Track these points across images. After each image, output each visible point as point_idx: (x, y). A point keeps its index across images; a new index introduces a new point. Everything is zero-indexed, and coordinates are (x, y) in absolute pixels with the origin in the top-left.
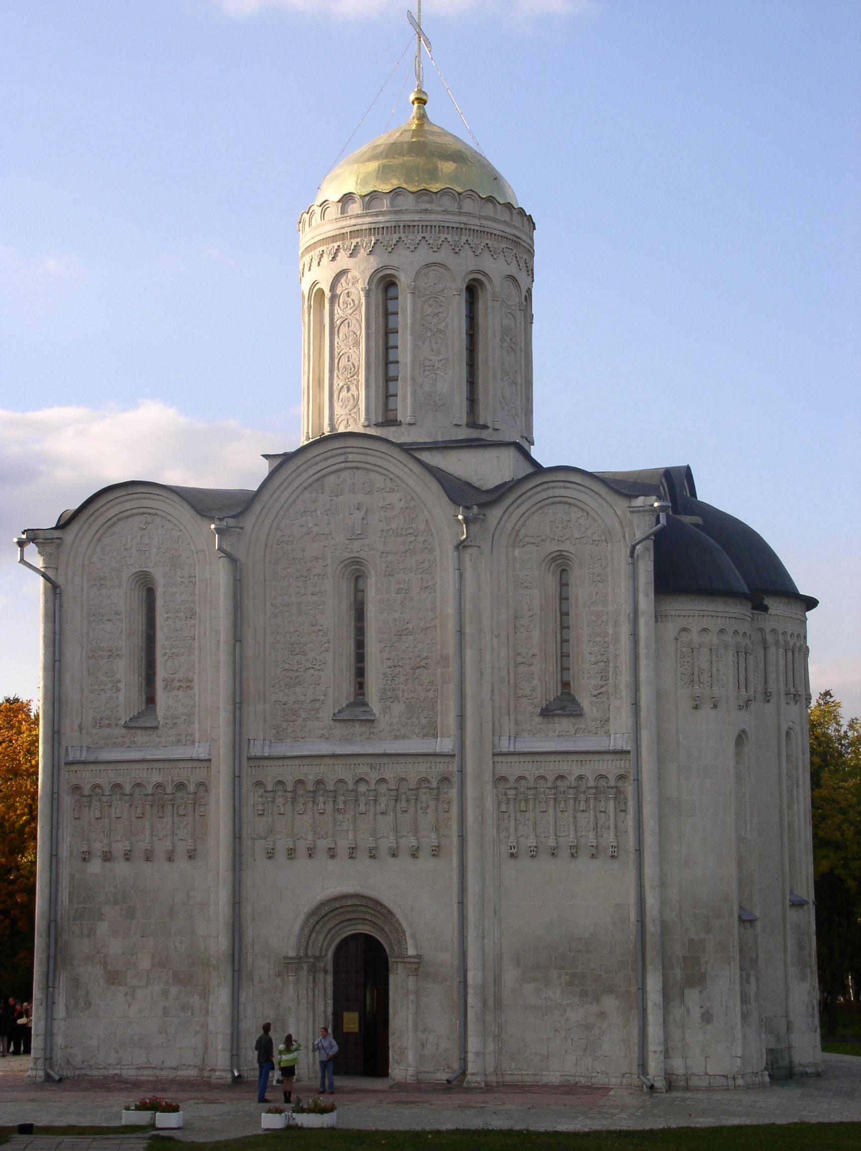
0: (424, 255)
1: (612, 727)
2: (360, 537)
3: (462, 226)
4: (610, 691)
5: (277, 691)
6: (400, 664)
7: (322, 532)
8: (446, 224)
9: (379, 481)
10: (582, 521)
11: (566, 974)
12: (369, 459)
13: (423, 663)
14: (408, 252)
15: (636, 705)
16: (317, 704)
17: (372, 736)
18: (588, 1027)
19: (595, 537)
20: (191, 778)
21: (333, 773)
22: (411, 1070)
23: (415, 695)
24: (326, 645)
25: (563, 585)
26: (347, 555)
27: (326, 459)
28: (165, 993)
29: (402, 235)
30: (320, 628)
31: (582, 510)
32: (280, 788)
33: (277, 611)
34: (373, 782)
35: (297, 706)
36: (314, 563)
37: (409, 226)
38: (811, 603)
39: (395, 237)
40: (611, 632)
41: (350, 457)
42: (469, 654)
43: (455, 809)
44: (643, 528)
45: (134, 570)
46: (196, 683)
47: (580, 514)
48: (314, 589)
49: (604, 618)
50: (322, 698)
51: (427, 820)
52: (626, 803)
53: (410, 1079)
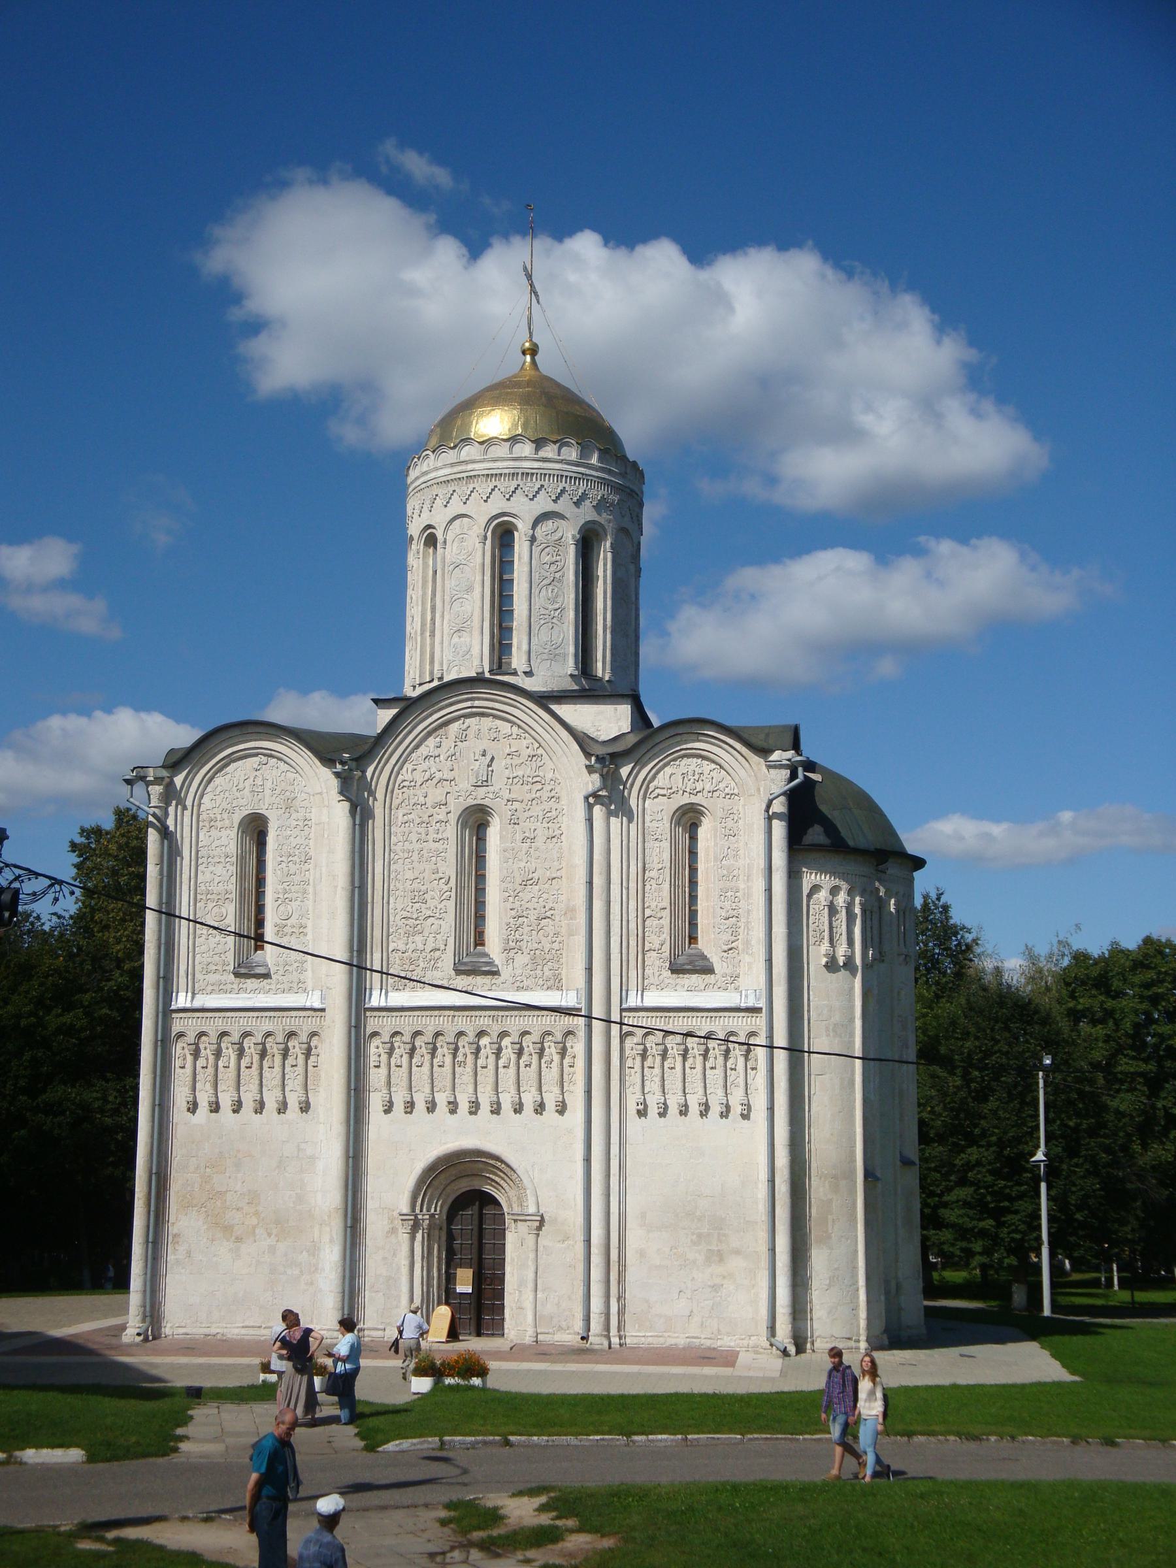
0: (543, 504)
1: (743, 982)
4: (740, 947)
6: (525, 913)
8: (565, 474)
9: (505, 728)
10: (714, 774)
11: (693, 1234)
12: (497, 706)
13: (548, 914)
15: (769, 961)
16: (438, 953)
18: (716, 1288)
19: (727, 791)
20: (304, 1026)
21: (450, 1025)
22: (530, 1332)
23: (540, 946)
25: (693, 838)
26: (471, 802)
28: (272, 1250)
29: (519, 482)
30: (441, 875)
31: (713, 762)
32: (397, 1038)
34: (495, 1035)
38: (918, 863)
40: (742, 886)
41: (477, 703)
42: (598, 905)
43: (580, 1063)
44: (778, 781)
45: (247, 812)
46: (309, 930)
47: (713, 766)
49: (735, 873)
51: (551, 1075)
52: (756, 1060)
53: (528, 1339)
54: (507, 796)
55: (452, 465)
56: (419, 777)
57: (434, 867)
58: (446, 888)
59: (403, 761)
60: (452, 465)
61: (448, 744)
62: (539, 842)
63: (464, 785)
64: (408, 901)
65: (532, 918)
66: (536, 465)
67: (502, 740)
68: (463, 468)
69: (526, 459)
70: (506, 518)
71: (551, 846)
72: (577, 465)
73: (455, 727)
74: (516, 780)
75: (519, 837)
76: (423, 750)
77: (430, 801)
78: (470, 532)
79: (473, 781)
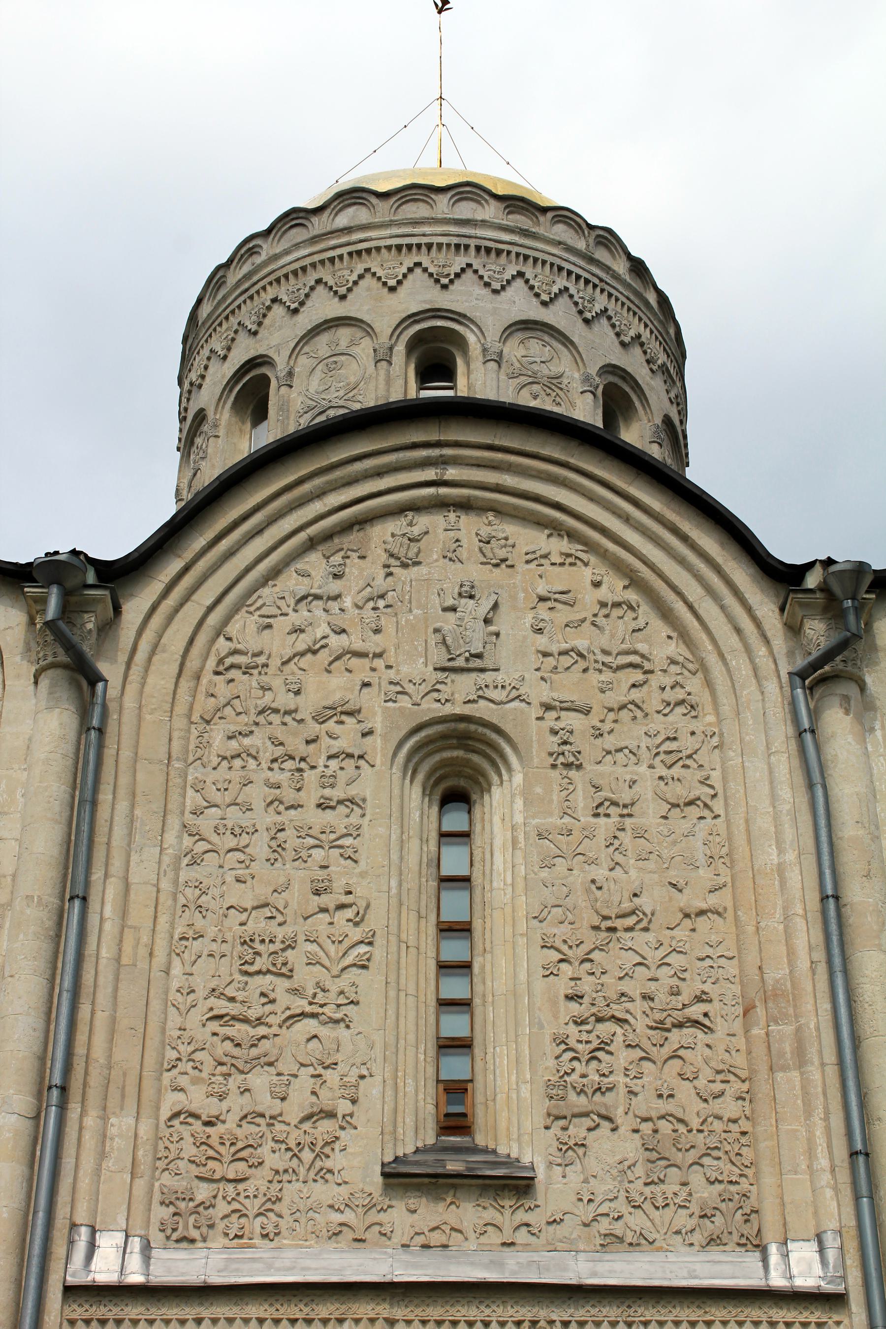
2: (477, 663)
3: (597, 281)
5: (183, 1081)
7: (358, 646)
14: (486, 292)
16: (326, 1126)
17: (522, 1236)
24: (363, 949)
26: (431, 708)
27: (379, 473)
33: (202, 846)
35: (248, 1128)
36: (331, 724)
37: (488, 250)
39: (460, 261)
41: (452, 473)
48: (327, 792)
50: (344, 1107)
54: (545, 694)
55: (314, 240)
56: (278, 643)
57: (322, 874)
58: (356, 934)
59: (241, 598)
60: (314, 240)
61: (364, 571)
62: (649, 814)
63: (416, 666)
64: (228, 968)
65: (640, 1024)
66: (506, 237)
67: (521, 567)
68: (344, 239)
69: (484, 223)
70: (440, 323)
71: (685, 826)
72: (591, 260)
73: (383, 533)
74: (566, 661)
75: (582, 800)
76: (291, 583)
77: (308, 704)
78: (355, 350)
79: (439, 656)
